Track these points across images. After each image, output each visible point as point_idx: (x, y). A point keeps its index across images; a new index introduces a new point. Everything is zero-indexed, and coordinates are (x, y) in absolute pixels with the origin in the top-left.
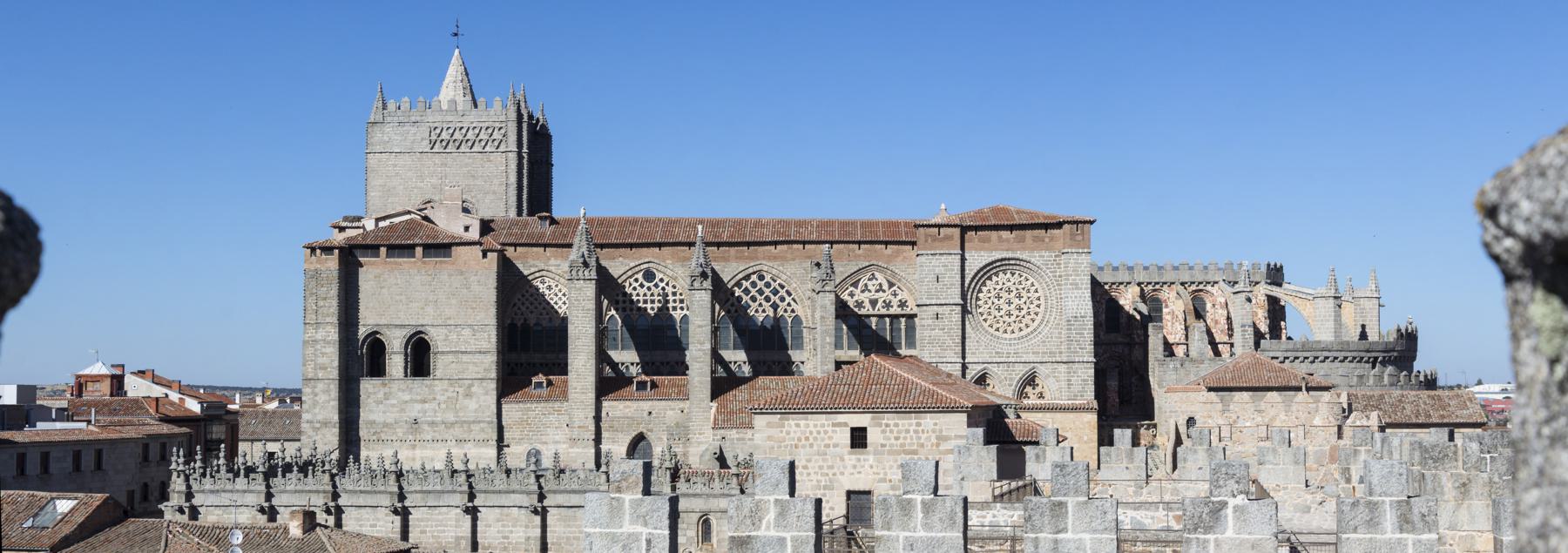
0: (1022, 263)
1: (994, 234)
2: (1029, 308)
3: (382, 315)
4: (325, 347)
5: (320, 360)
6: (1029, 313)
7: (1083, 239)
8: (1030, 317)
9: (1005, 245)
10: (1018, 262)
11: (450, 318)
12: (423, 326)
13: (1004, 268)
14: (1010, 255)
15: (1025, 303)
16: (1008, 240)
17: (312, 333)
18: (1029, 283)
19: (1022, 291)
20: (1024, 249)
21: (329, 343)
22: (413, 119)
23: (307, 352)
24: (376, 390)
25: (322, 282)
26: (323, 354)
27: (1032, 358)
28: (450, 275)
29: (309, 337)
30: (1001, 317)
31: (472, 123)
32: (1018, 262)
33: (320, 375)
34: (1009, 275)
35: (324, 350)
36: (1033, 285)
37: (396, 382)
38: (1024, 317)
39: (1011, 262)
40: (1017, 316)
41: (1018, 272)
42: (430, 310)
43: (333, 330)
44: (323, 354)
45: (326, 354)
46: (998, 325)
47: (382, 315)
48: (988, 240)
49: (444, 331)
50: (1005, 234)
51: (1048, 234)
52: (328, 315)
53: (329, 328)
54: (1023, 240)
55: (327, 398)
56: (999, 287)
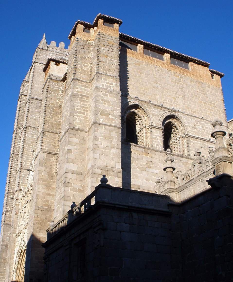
3: (142, 94)
4: (107, 95)
5: (101, 106)
11: (195, 112)
12: (176, 111)
17: (81, 89)
21: (111, 92)
23: (76, 104)
24: (139, 157)
25: (105, 43)
26: (105, 101)
28: (192, 81)
29: (77, 91)
33: (101, 121)
35: (105, 98)
37: (156, 153)
42: (180, 100)
43: (114, 83)
44: (105, 101)
45: (108, 101)
47: (142, 94)
49: (192, 120)
52: (109, 70)
53: (110, 80)
55: (109, 145)
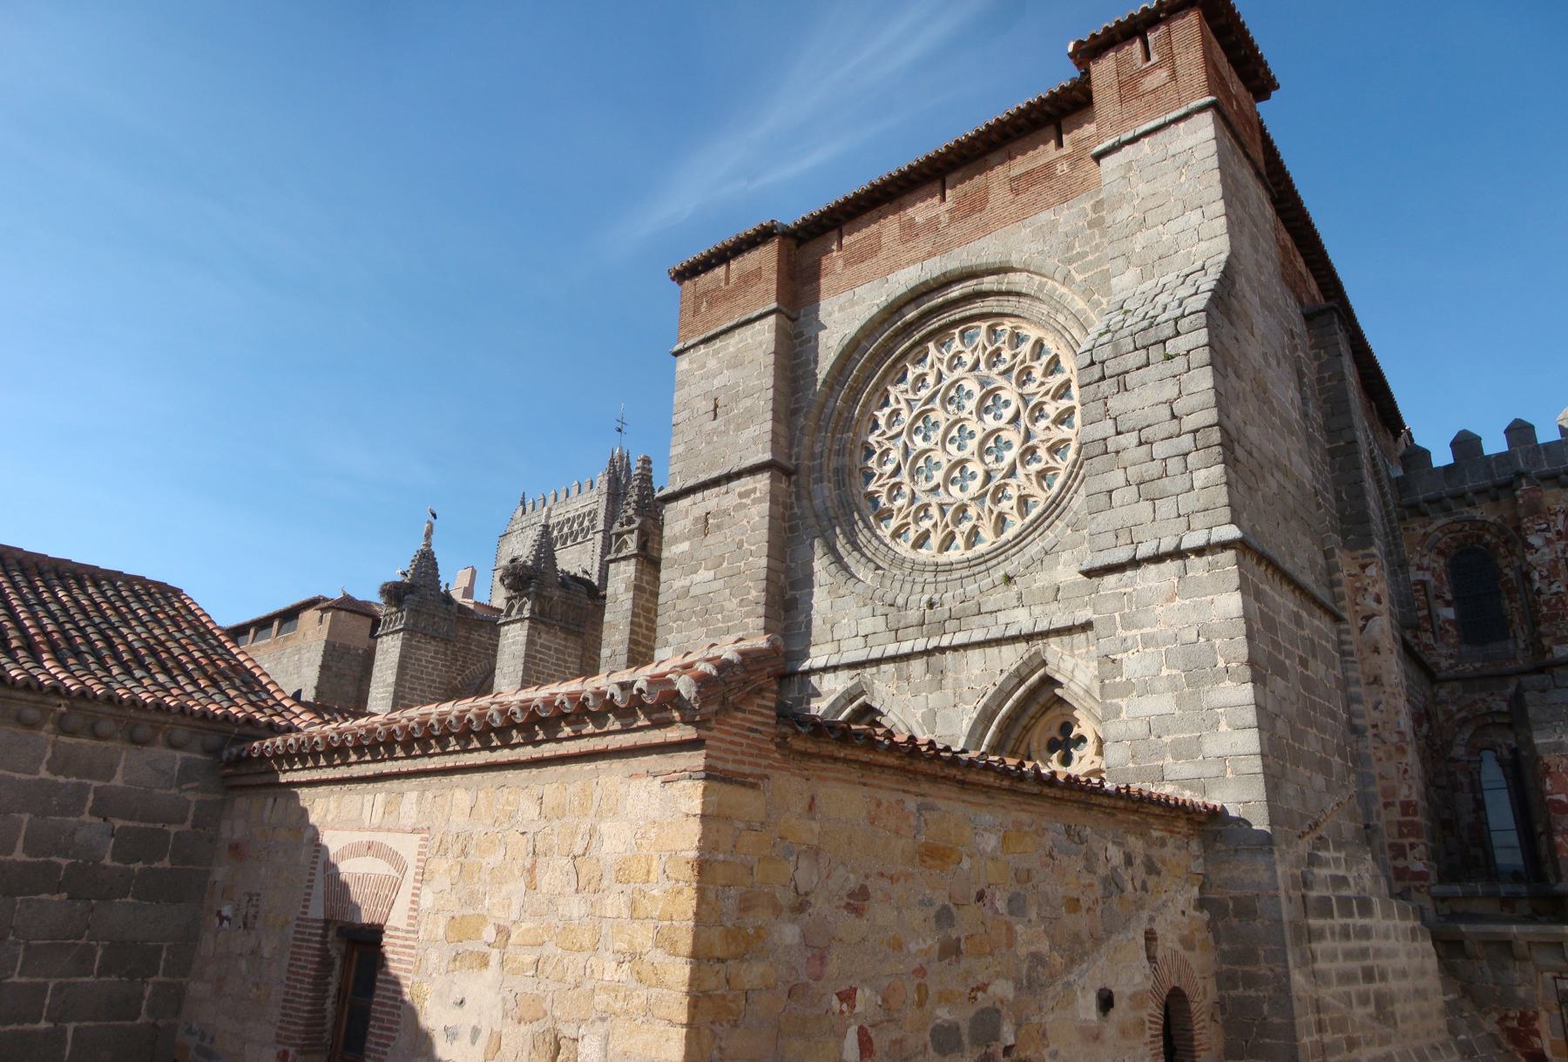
0: (989, 283)
1: (889, 227)
2: (1028, 435)
6: (1029, 453)
7: (1174, 76)
8: (1034, 467)
9: (923, 244)
10: (969, 286)
13: (935, 324)
14: (934, 268)
15: (1015, 419)
16: (932, 225)
18: (1026, 348)
19: (1001, 382)
20: (985, 230)
22: (533, 522)
27: (1022, 620)
30: (935, 489)
31: (577, 510)
32: (969, 286)
34: (957, 345)
36: (1039, 346)
38: (1012, 472)
39: (956, 292)
40: (988, 477)
41: (984, 325)
46: (926, 524)
48: (874, 250)
50: (923, 211)
51: (1067, 148)
54: (975, 205)
56: (924, 393)
